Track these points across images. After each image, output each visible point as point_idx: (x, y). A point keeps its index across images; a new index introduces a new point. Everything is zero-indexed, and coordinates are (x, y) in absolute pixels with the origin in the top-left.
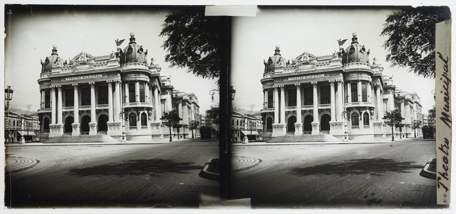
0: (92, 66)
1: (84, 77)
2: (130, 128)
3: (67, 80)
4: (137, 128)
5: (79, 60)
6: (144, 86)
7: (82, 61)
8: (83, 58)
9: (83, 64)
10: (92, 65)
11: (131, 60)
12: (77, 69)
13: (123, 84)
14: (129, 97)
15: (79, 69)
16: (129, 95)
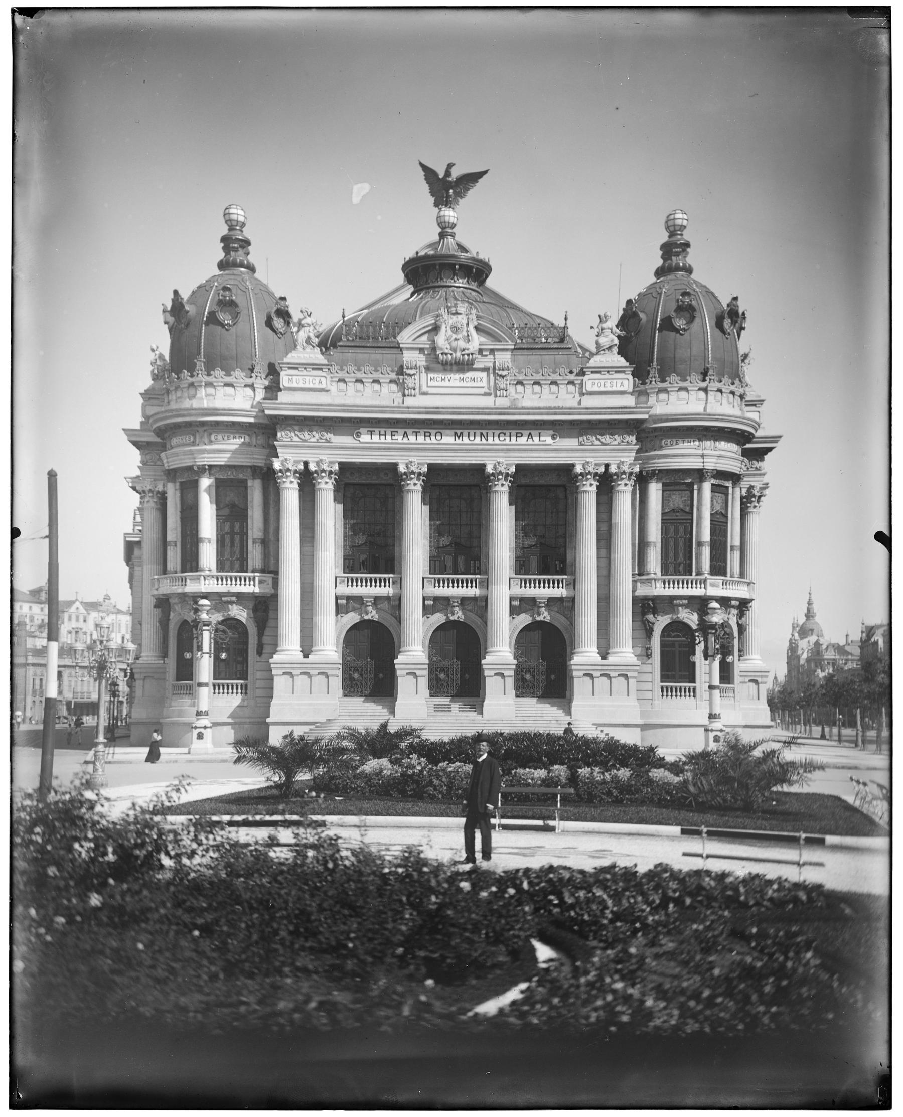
0: (502, 383)
1: (459, 432)
2: (662, 691)
3: (365, 438)
4: (694, 692)
5: (441, 340)
6: (727, 495)
7: (455, 351)
8: (459, 336)
9: (454, 368)
10: (502, 377)
11: (681, 367)
12: (424, 389)
13: (642, 480)
14: (659, 545)
15: (431, 391)
16: (659, 537)
